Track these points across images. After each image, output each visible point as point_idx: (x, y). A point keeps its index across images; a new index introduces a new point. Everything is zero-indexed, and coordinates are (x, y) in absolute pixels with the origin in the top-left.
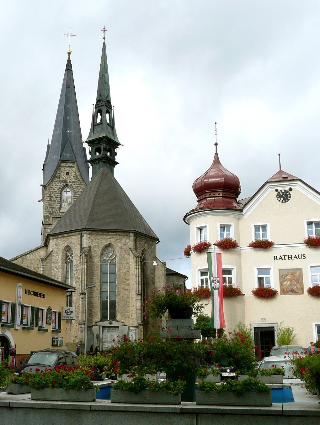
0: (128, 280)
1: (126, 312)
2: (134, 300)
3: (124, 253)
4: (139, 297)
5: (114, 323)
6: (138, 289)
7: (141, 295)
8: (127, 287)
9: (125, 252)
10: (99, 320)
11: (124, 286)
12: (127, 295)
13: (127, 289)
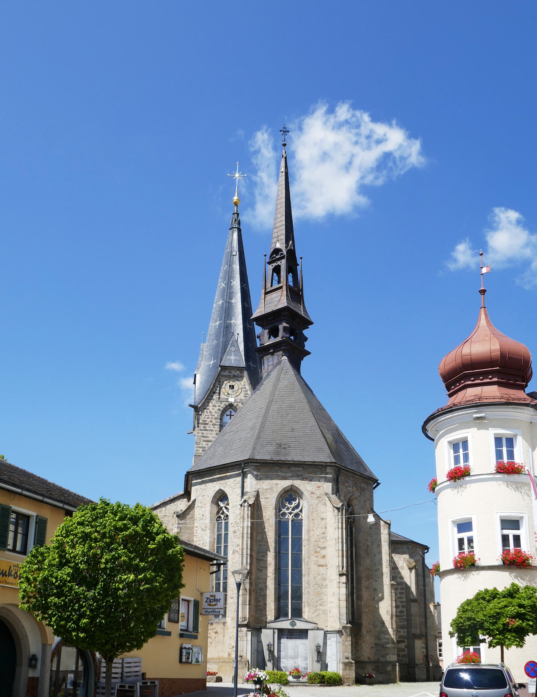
0: (324, 548)
1: (320, 605)
2: (335, 584)
3: (316, 501)
4: (344, 579)
5: (300, 625)
6: (341, 564)
7: (347, 575)
8: (322, 561)
9: (318, 501)
10: (273, 619)
11: (316, 559)
12: (323, 574)
13: (322, 564)
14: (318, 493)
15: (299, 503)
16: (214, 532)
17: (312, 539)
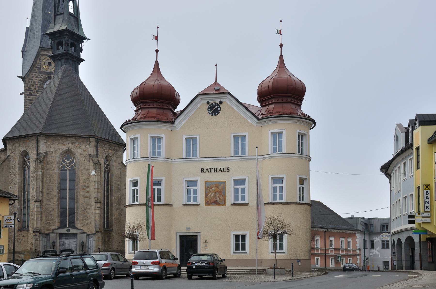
0: (88, 187)
8: (87, 195)
14: (85, 154)
15: (73, 159)
16: (21, 176)
17: (81, 182)
